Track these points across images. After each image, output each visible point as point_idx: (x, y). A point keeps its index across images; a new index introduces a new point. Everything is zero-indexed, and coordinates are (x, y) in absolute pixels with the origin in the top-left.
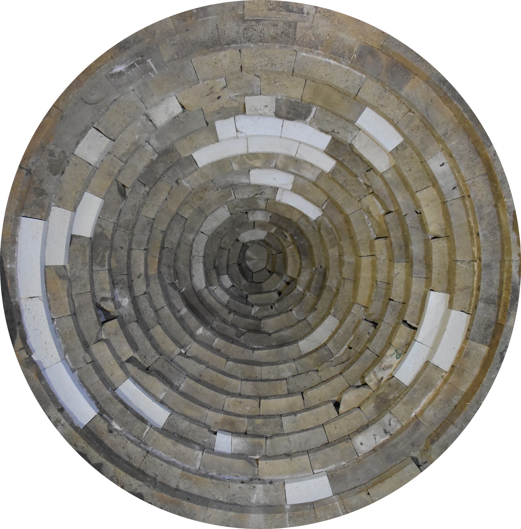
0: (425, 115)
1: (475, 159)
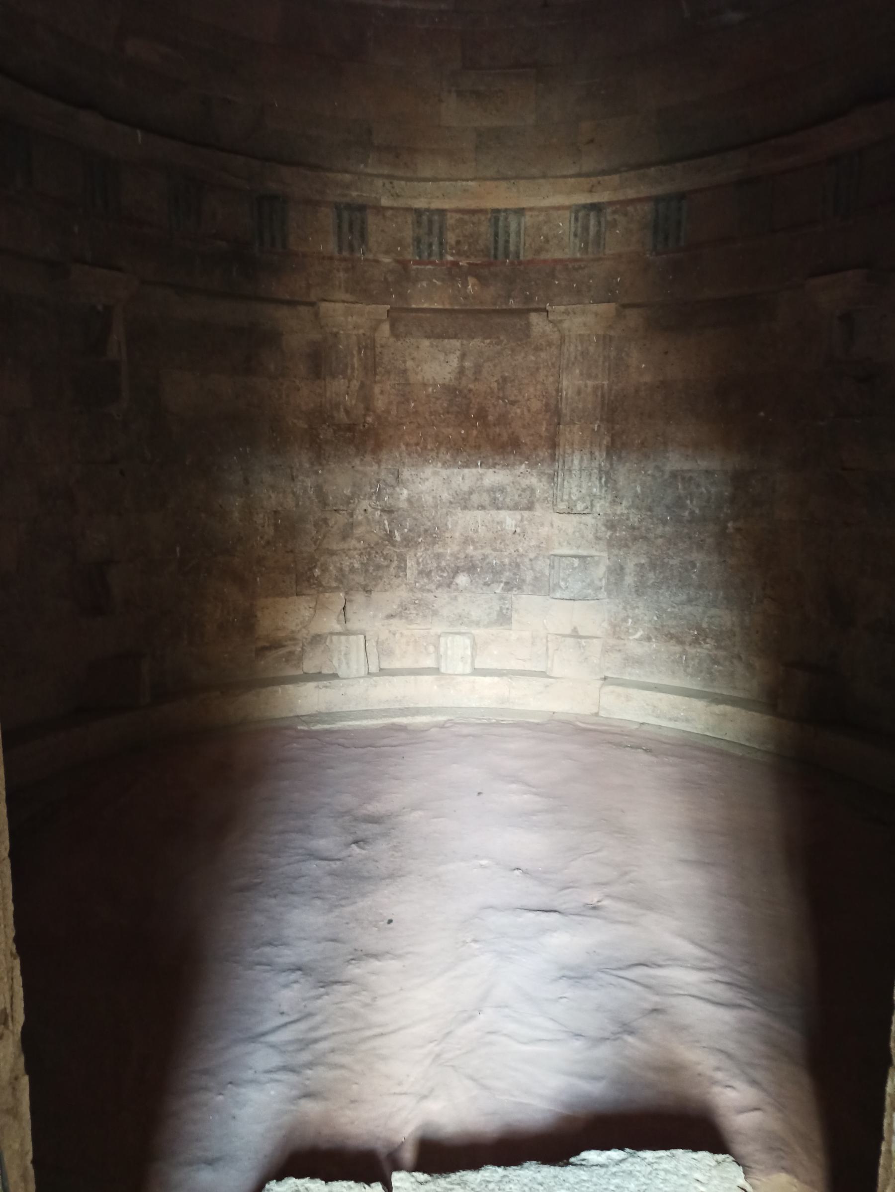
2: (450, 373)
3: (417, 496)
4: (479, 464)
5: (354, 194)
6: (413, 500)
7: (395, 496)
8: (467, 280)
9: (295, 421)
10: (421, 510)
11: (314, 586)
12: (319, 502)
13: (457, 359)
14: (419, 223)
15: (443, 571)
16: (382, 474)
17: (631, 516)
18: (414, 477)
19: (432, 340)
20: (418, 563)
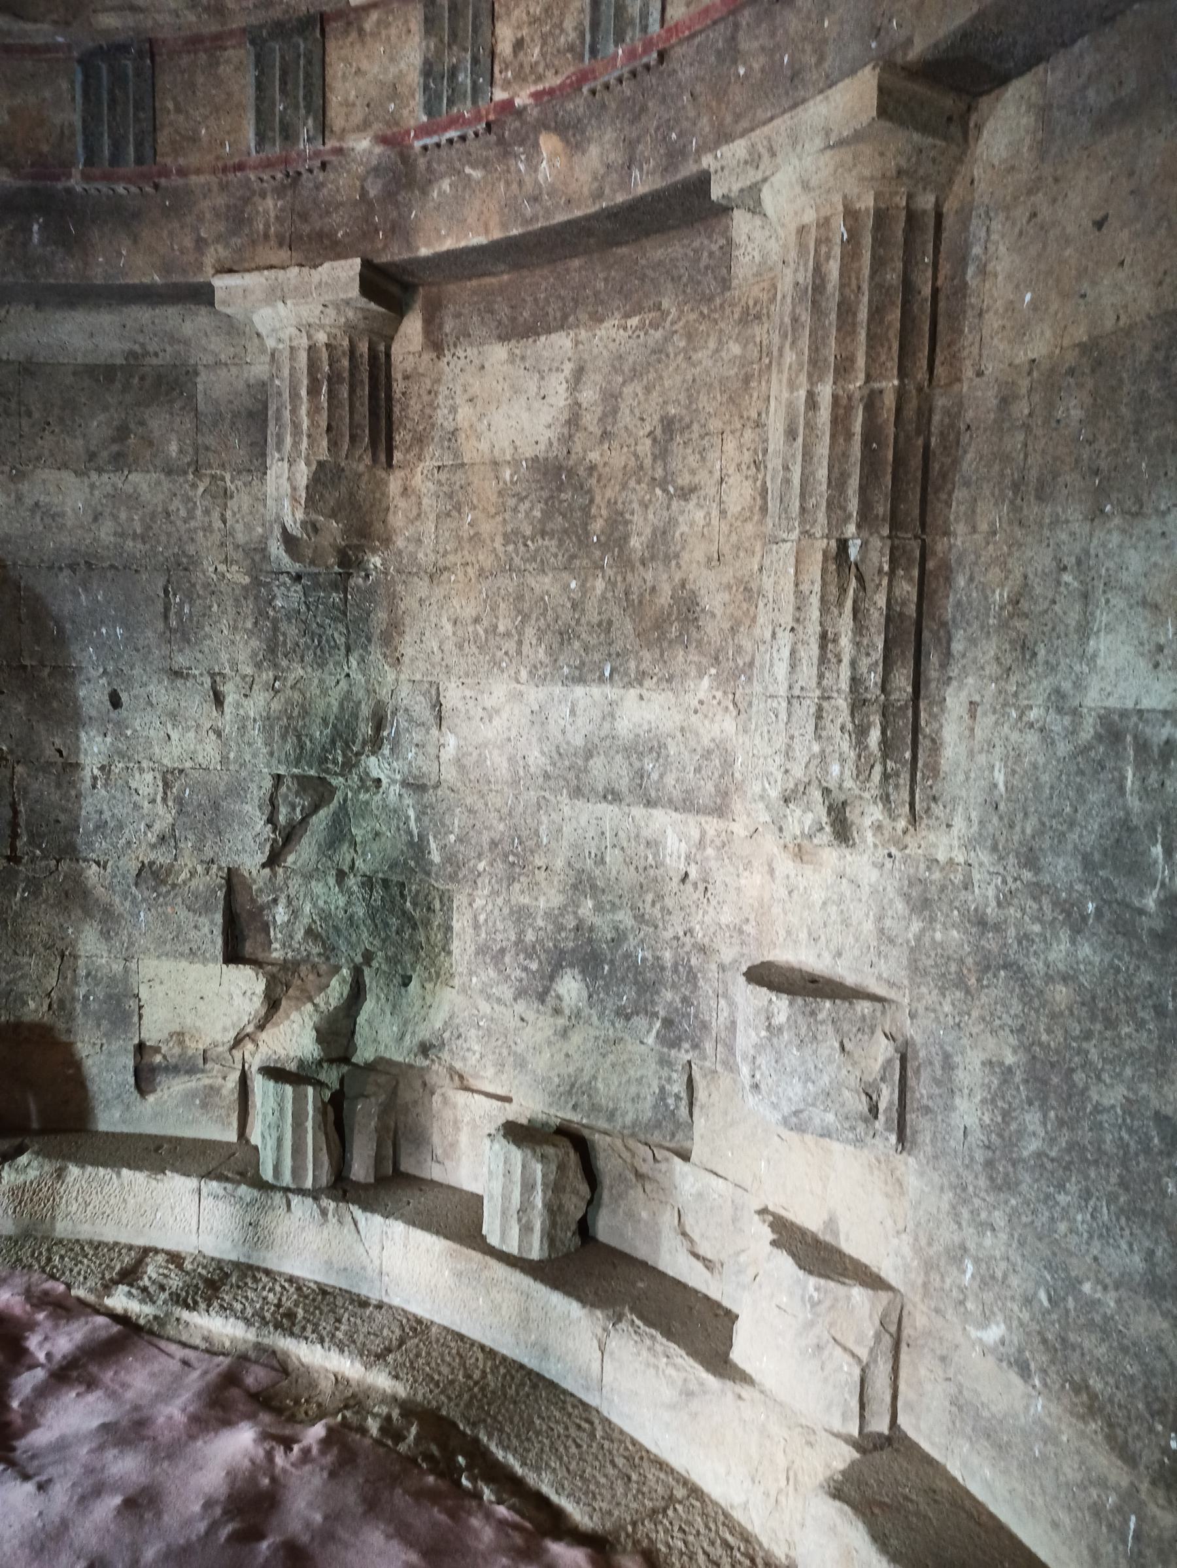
2: (549, 426)
3: (475, 753)
4: (607, 674)
6: (468, 762)
7: (432, 750)
8: (536, 145)
9: (222, 568)
10: (485, 789)
12: (272, 754)
13: (564, 385)
16: (403, 695)
17: (976, 876)
18: (471, 703)
19: (513, 342)
20: (476, 926)
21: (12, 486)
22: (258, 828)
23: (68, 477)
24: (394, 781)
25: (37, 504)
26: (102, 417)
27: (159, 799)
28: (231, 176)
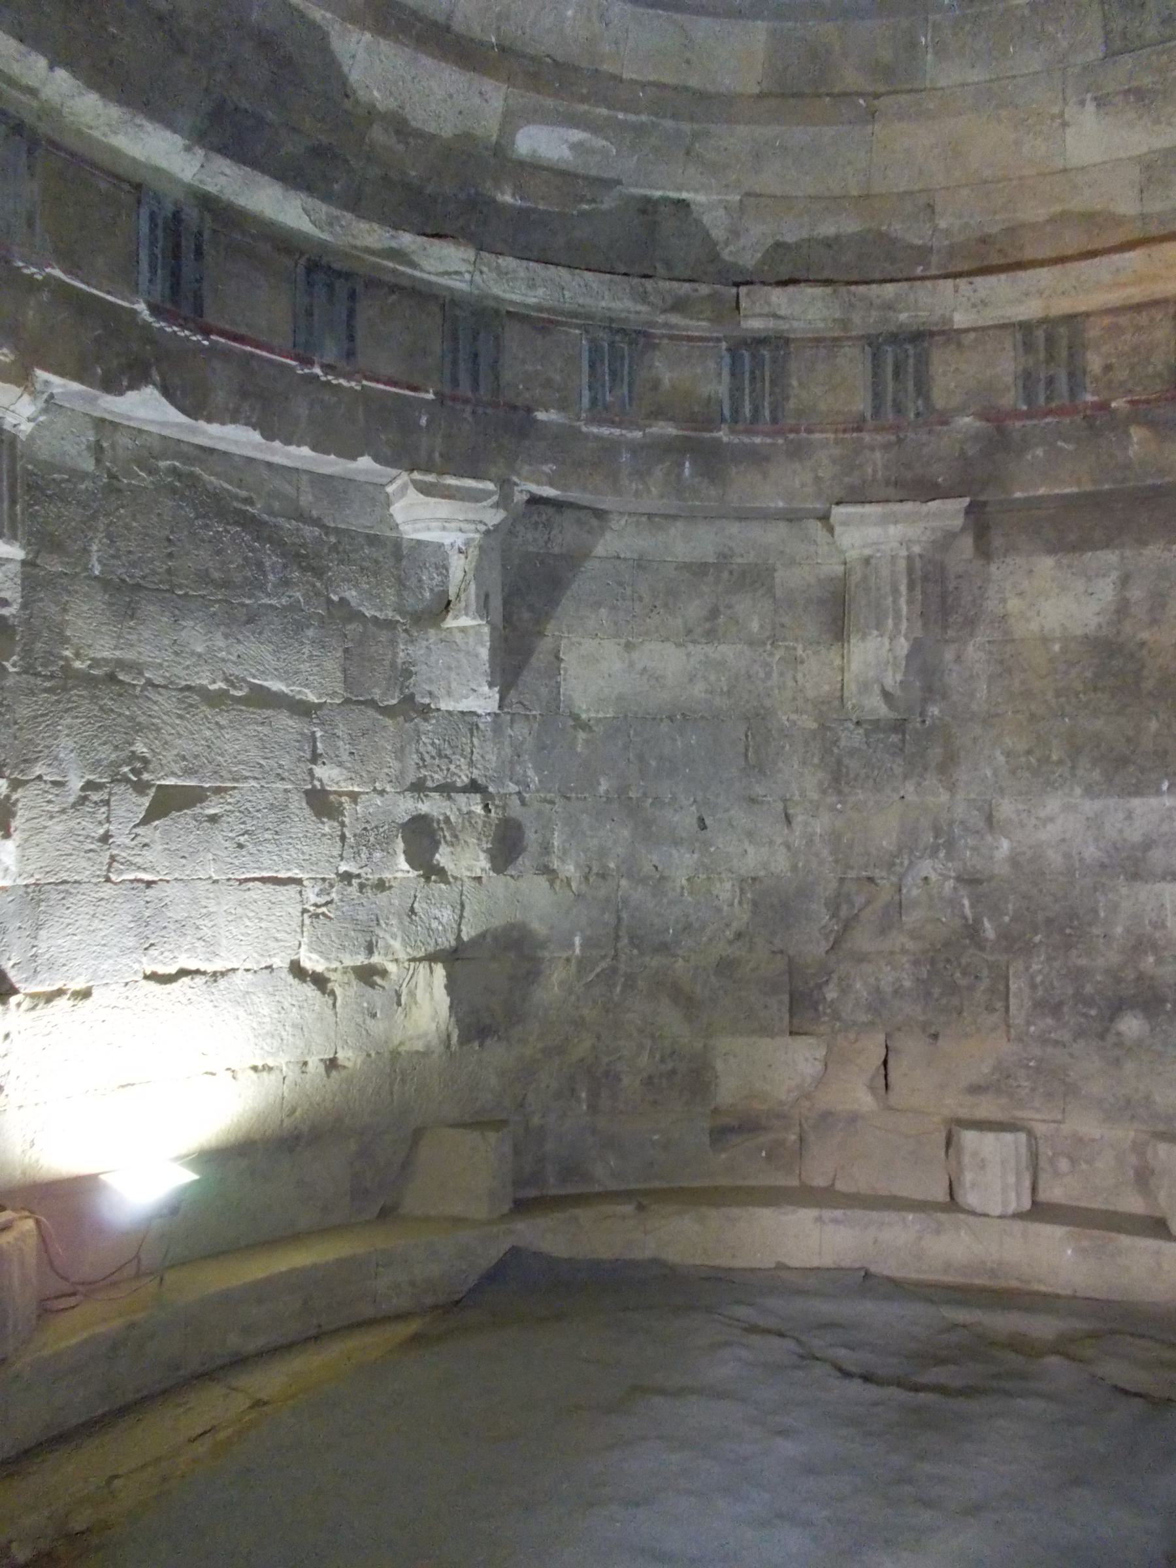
0: (678, 17)
1: (499, 28)
5: (903, 317)
9: (794, 717)
11: (826, 1019)
12: (836, 861)
13: (1112, 586)
14: (1028, 347)
15: (1091, 1007)
16: (959, 811)
18: (1024, 815)
19: (1060, 555)
20: (1033, 986)
21: (626, 655)
22: (824, 922)
23: (669, 648)
24: (947, 878)
25: (645, 669)
26: (697, 602)
27: (736, 901)
28: (847, 436)
